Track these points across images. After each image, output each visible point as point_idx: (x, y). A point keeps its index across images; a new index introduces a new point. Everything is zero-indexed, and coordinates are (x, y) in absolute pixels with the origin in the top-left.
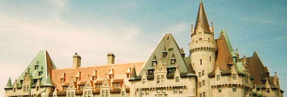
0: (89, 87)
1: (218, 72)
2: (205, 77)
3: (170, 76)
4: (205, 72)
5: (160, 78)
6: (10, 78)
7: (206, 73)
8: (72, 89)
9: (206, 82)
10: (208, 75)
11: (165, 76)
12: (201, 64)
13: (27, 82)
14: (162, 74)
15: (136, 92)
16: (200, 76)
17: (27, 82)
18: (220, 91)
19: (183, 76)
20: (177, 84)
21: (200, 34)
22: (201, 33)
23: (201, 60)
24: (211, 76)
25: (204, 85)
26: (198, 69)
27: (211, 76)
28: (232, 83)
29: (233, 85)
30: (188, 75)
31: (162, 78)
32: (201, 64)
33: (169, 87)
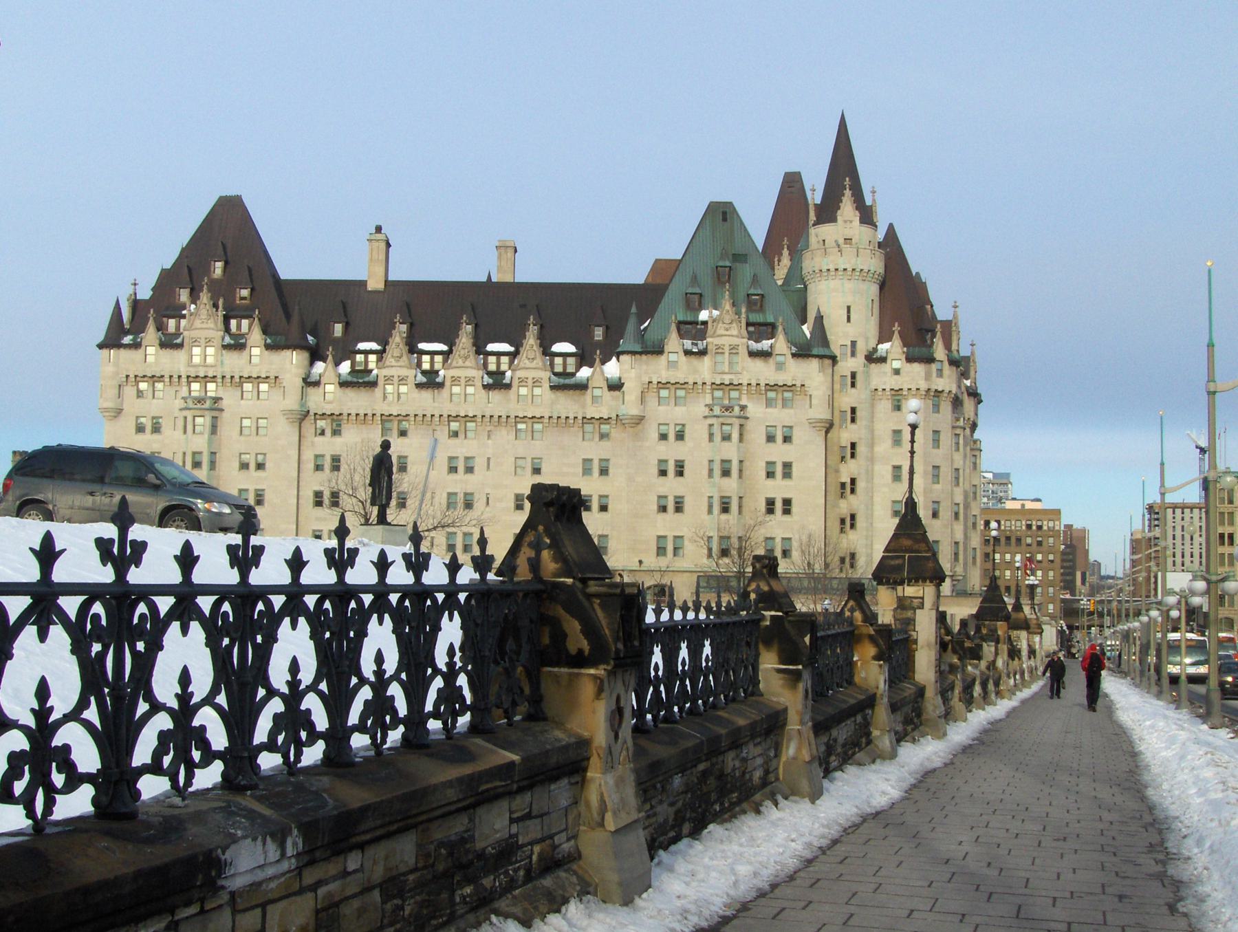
0: (468, 363)
5: (727, 354)
6: (118, 301)
8: (399, 364)
9: (859, 377)
12: (849, 320)
13: (204, 326)
14: (736, 341)
17: (204, 326)
20: (781, 378)
22: (851, 222)
23: (849, 308)
26: (839, 335)
28: (934, 387)
29: (936, 390)
30: (815, 352)
31: (730, 353)
32: (849, 320)
33: (754, 383)
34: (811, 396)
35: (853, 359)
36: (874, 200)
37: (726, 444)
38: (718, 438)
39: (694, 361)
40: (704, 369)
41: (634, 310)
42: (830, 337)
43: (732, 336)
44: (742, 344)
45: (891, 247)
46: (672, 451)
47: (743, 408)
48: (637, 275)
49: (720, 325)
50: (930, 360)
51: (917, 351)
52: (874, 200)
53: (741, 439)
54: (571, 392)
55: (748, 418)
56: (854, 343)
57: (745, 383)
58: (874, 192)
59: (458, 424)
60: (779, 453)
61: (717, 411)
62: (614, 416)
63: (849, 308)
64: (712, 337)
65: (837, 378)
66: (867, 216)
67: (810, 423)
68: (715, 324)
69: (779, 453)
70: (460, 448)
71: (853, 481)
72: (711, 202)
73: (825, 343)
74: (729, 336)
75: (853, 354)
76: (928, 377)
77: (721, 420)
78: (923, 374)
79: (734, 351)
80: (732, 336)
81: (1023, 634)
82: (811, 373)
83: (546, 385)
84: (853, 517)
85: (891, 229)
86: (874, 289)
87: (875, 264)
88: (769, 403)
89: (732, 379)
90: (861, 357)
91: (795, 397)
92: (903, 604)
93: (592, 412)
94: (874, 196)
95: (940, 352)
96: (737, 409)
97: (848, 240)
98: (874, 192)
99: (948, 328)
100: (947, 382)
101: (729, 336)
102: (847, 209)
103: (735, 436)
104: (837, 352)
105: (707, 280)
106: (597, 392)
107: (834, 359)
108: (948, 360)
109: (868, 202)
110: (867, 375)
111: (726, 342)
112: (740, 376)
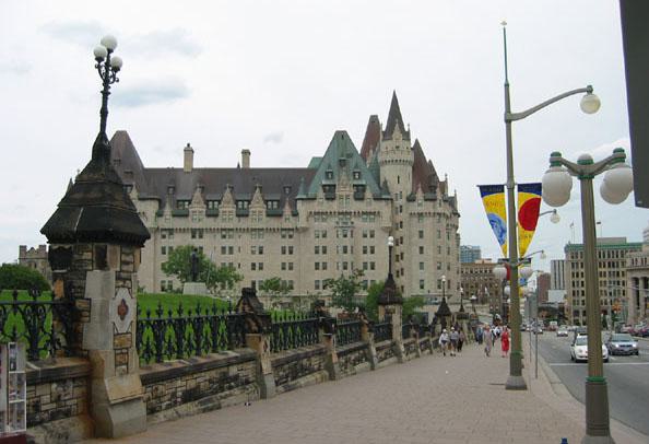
1: (420, 195)
2: (402, 201)
3: (359, 197)
7: (405, 195)
9: (404, 208)
19: (377, 199)
20: (369, 209)
24: (411, 199)
26: (395, 188)
27: (411, 199)
38: (341, 236)
39: (330, 203)
40: (334, 206)
41: (303, 179)
42: (390, 190)
45: (417, 149)
46: (321, 242)
48: (305, 164)
50: (435, 200)
51: (429, 196)
53: (352, 236)
59: (225, 232)
60: (368, 242)
66: (407, 135)
69: (368, 242)
70: (227, 243)
71: (402, 254)
73: (389, 193)
76: (434, 207)
81: (464, 321)
82: (384, 209)
83: (264, 214)
84: (402, 270)
85: (417, 142)
86: (410, 169)
87: (411, 157)
92: (388, 312)
93: (285, 226)
95: (439, 195)
96: (350, 224)
97: (397, 147)
99: (444, 185)
100: (444, 209)
102: (397, 134)
103: (349, 234)
104: (394, 197)
105: (335, 169)
110: (407, 208)
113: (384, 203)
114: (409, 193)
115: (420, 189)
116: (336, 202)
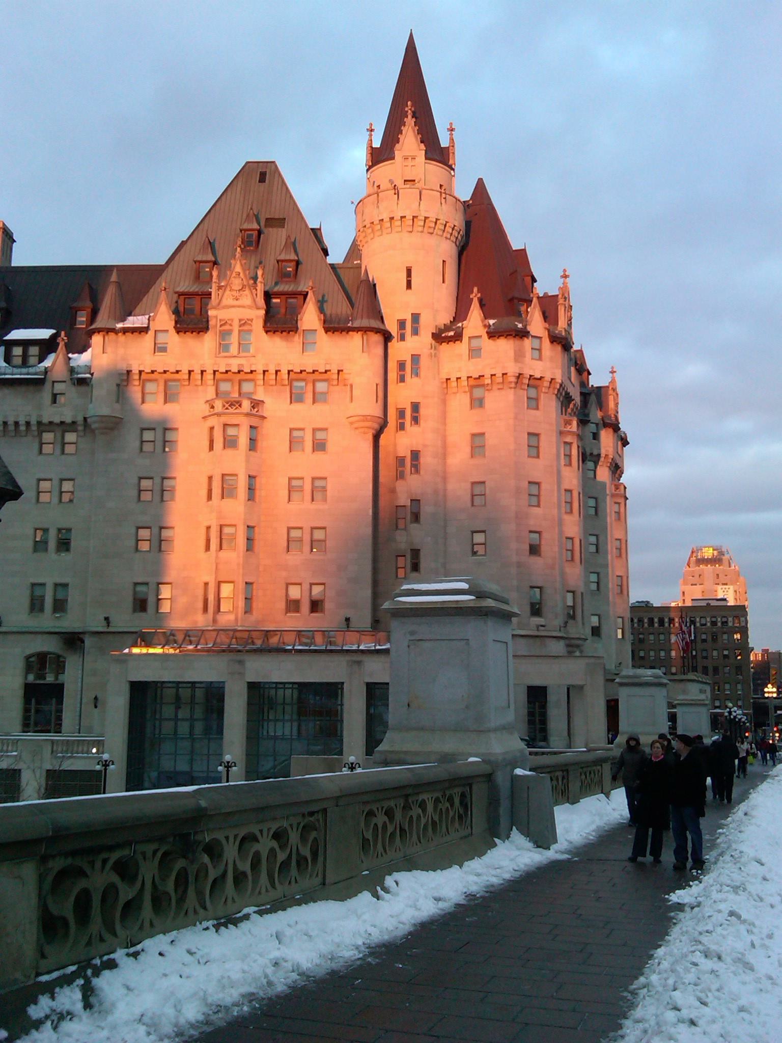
1: (474, 323)
4: (423, 320)
5: (235, 333)
7: (428, 325)
9: (424, 362)
10: (433, 333)
11: (258, 324)
12: (409, 285)
15: (118, 385)
16: (402, 338)
18: (477, 403)
20: (310, 361)
21: (410, 162)
25: (416, 373)
28: (527, 372)
31: (240, 331)
32: (409, 285)
34: (351, 386)
35: (415, 338)
36: (452, 140)
37: (230, 452)
43: (243, 307)
44: (257, 317)
47: (256, 404)
49: (228, 292)
52: (452, 140)
54: (23, 389)
55: (264, 418)
56: (416, 317)
57: (260, 369)
58: (452, 130)
61: (219, 405)
62: (80, 419)
63: (409, 271)
64: (214, 308)
65: (392, 365)
67: (351, 423)
68: (221, 292)
72: (248, 163)
74: (239, 307)
75: (415, 332)
76: (519, 356)
77: (224, 419)
78: (511, 354)
79: (246, 328)
80: (243, 307)
86: (446, 249)
88: (296, 398)
89: (242, 365)
90: (425, 338)
91: (332, 388)
93: (50, 414)
94: (451, 135)
95: (536, 324)
96: (246, 405)
98: (452, 130)
101: (239, 307)
102: (409, 141)
103: (243, 441)
104: (392, 327)
106: (59, 388)
107: (387, 337)
108: (549, 335)
109: (444, 143)
111: (234, 315)
112: (253, 360)
113: (356, 339)
114: (445, 318)
115: (475, 305)
116: (208, 341)
